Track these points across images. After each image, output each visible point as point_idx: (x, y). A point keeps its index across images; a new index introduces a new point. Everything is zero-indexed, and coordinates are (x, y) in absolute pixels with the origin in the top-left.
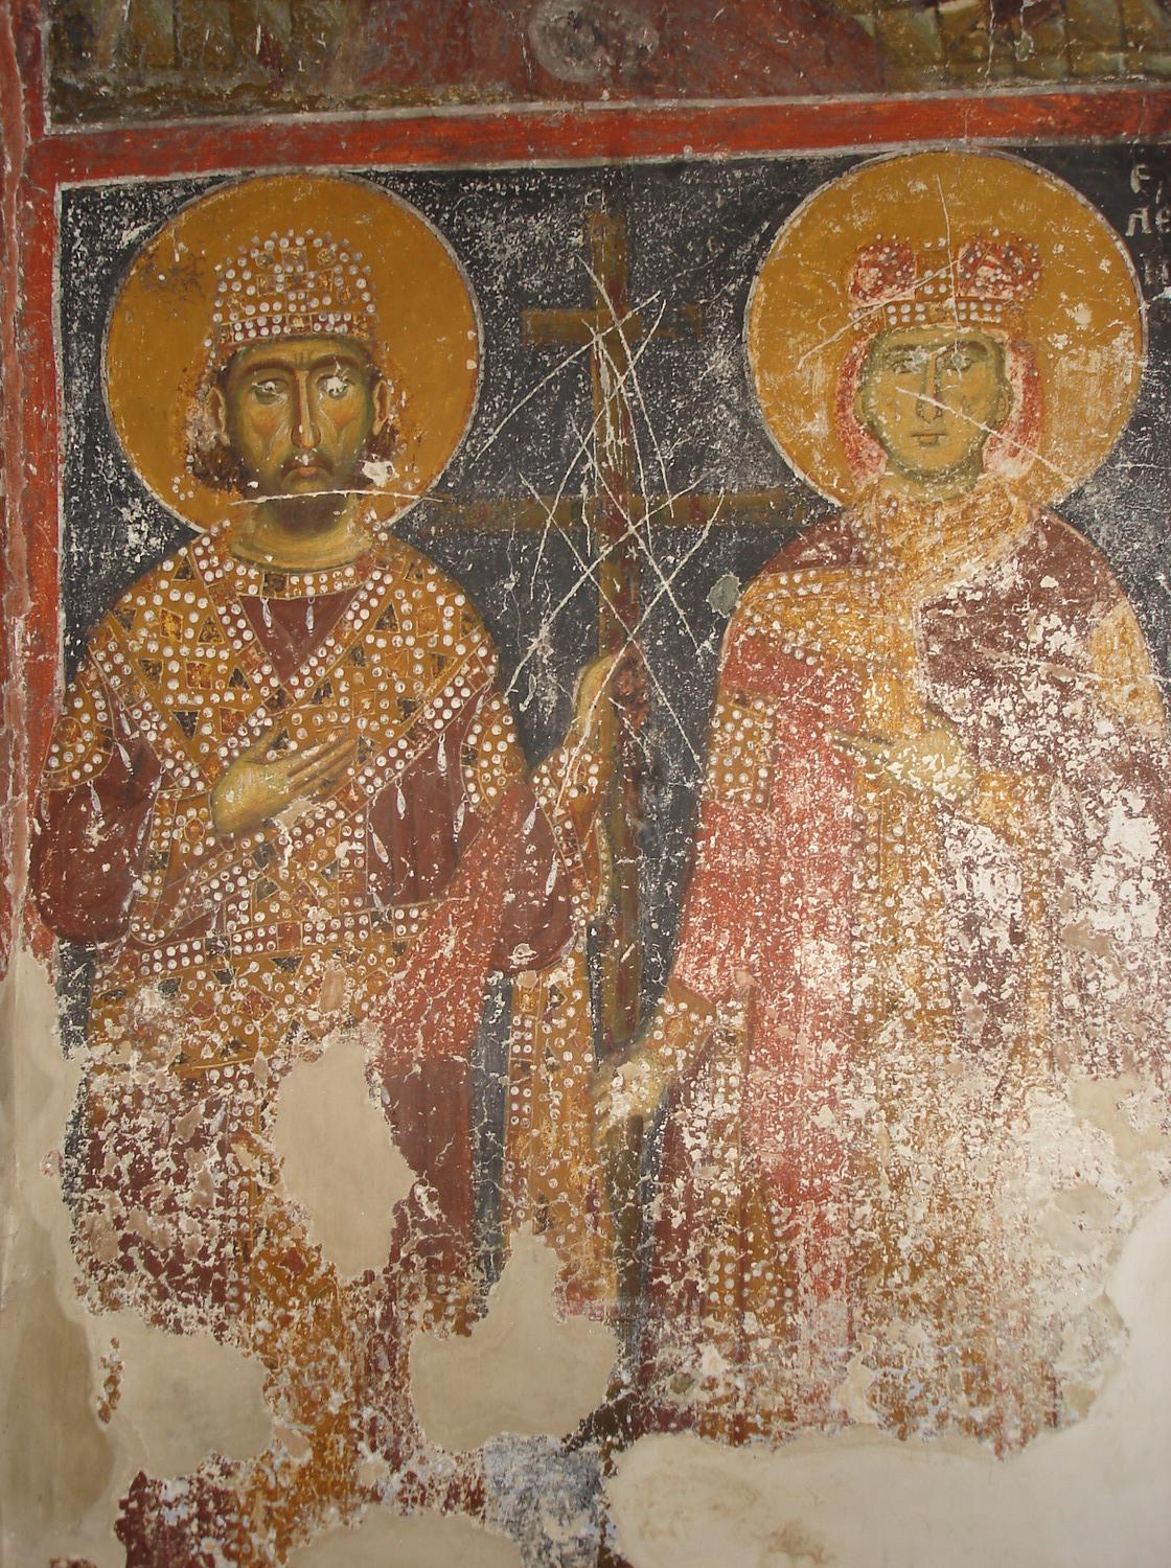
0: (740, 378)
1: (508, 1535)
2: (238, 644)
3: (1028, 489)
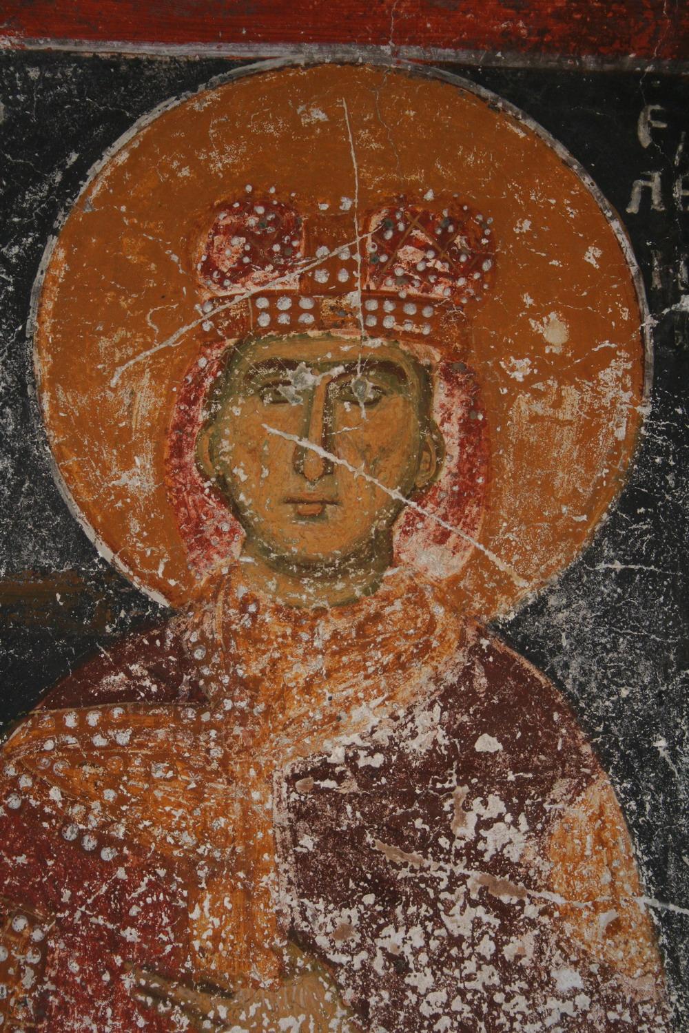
3: (461, 594)
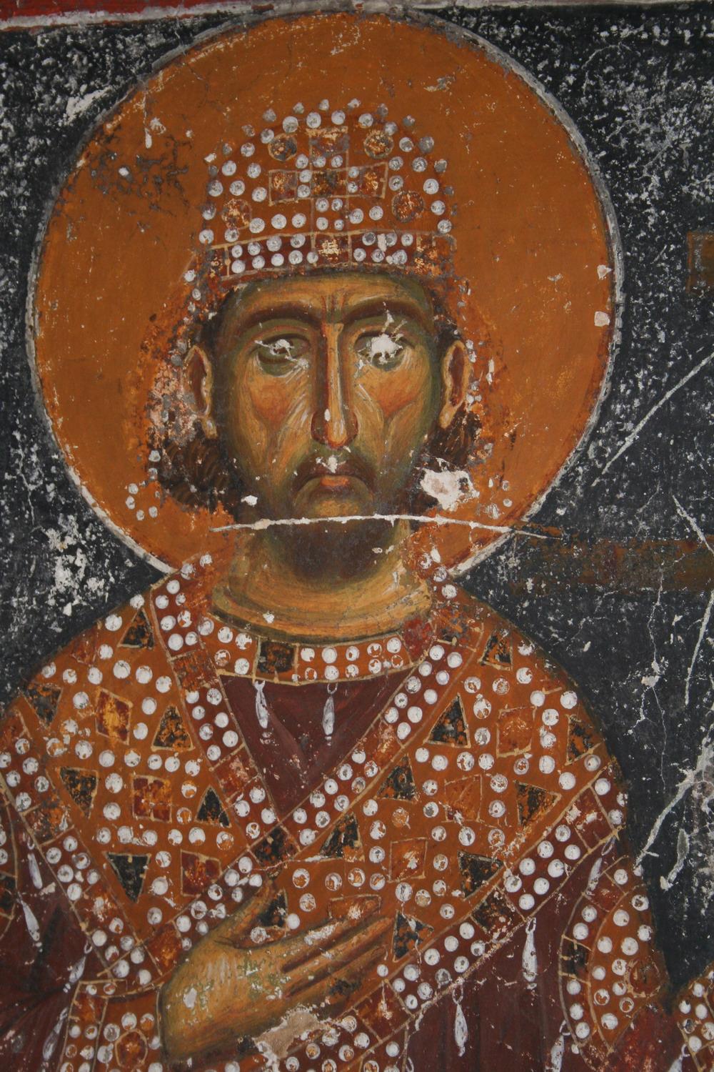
2: (214, 753)
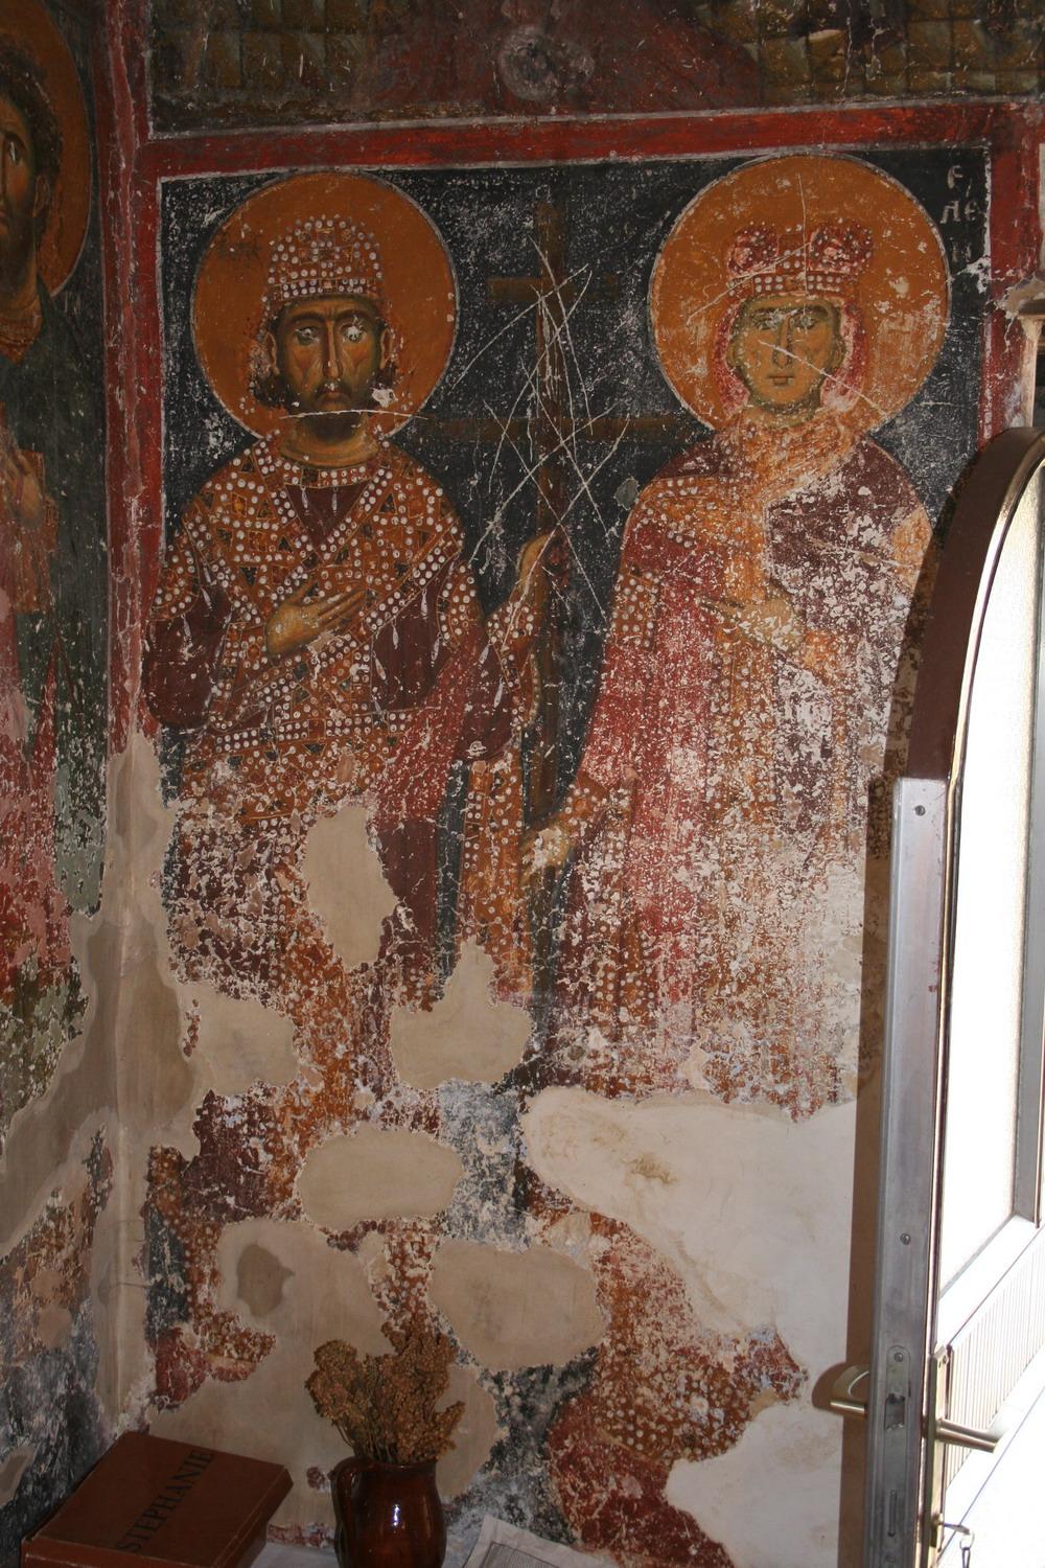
0: (644, 332)
1: (454, 1148)
2: (285, 520)
3: (854, 420)
